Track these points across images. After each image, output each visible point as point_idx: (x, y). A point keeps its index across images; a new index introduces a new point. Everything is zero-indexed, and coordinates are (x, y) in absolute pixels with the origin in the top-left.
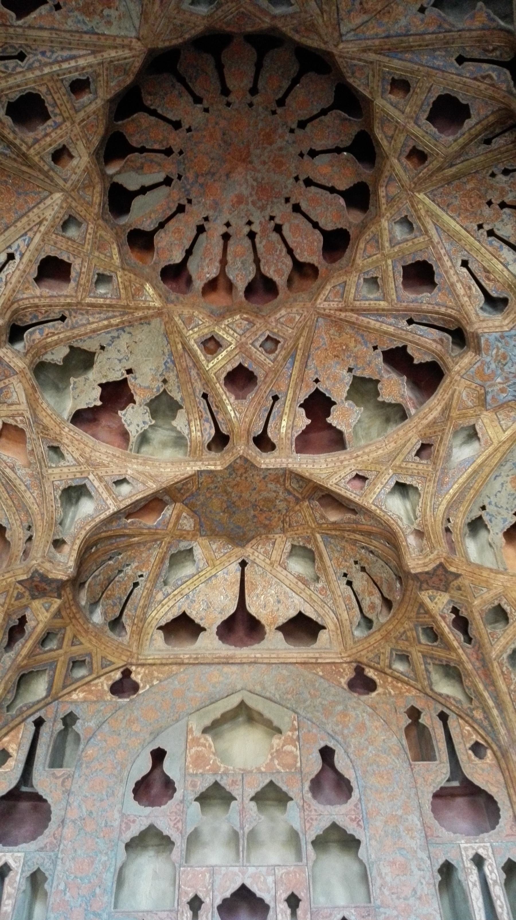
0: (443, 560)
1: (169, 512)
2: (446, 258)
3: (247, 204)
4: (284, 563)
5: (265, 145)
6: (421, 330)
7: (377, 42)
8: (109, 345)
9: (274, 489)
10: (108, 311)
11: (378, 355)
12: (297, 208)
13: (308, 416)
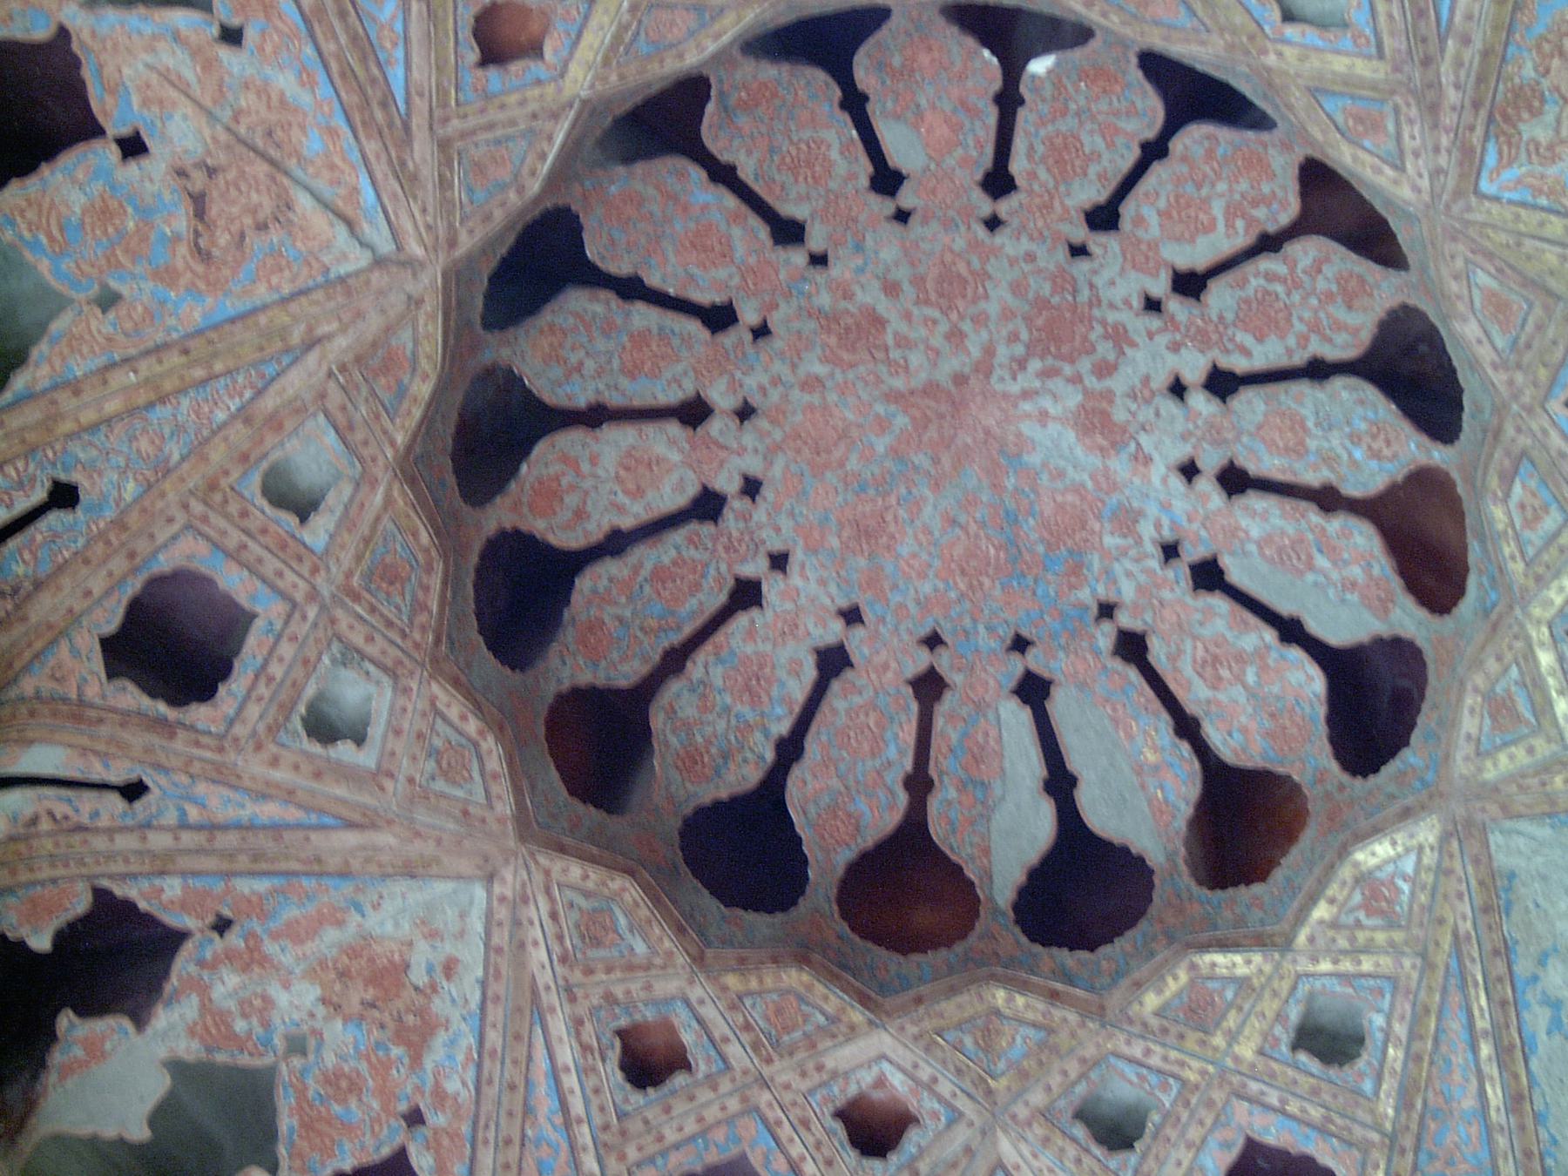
5: (890, 339)
7: (372, 147)
12: (1104, 218)
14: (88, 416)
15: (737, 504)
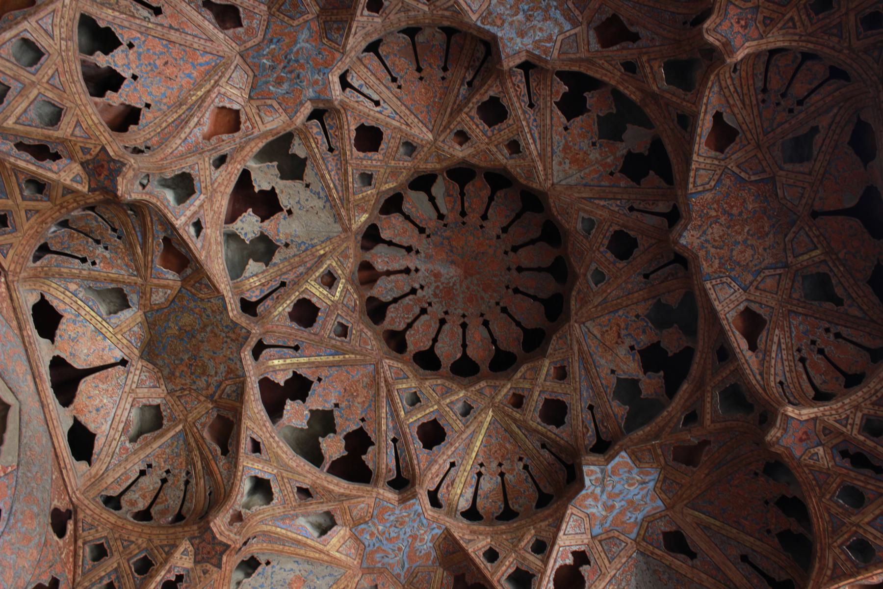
0: (233, 546)
1: (171, 277)
2: (453, 449)
3: (435, 282)
4: (138, 402)
6: (391, 452)
7: (586, 348)
8: (311, 191)
9: (219, 372)
10: (342, 186)
12: (443, 322)
13: (286, 382)
14: (641, 293)
15: (509, 249)
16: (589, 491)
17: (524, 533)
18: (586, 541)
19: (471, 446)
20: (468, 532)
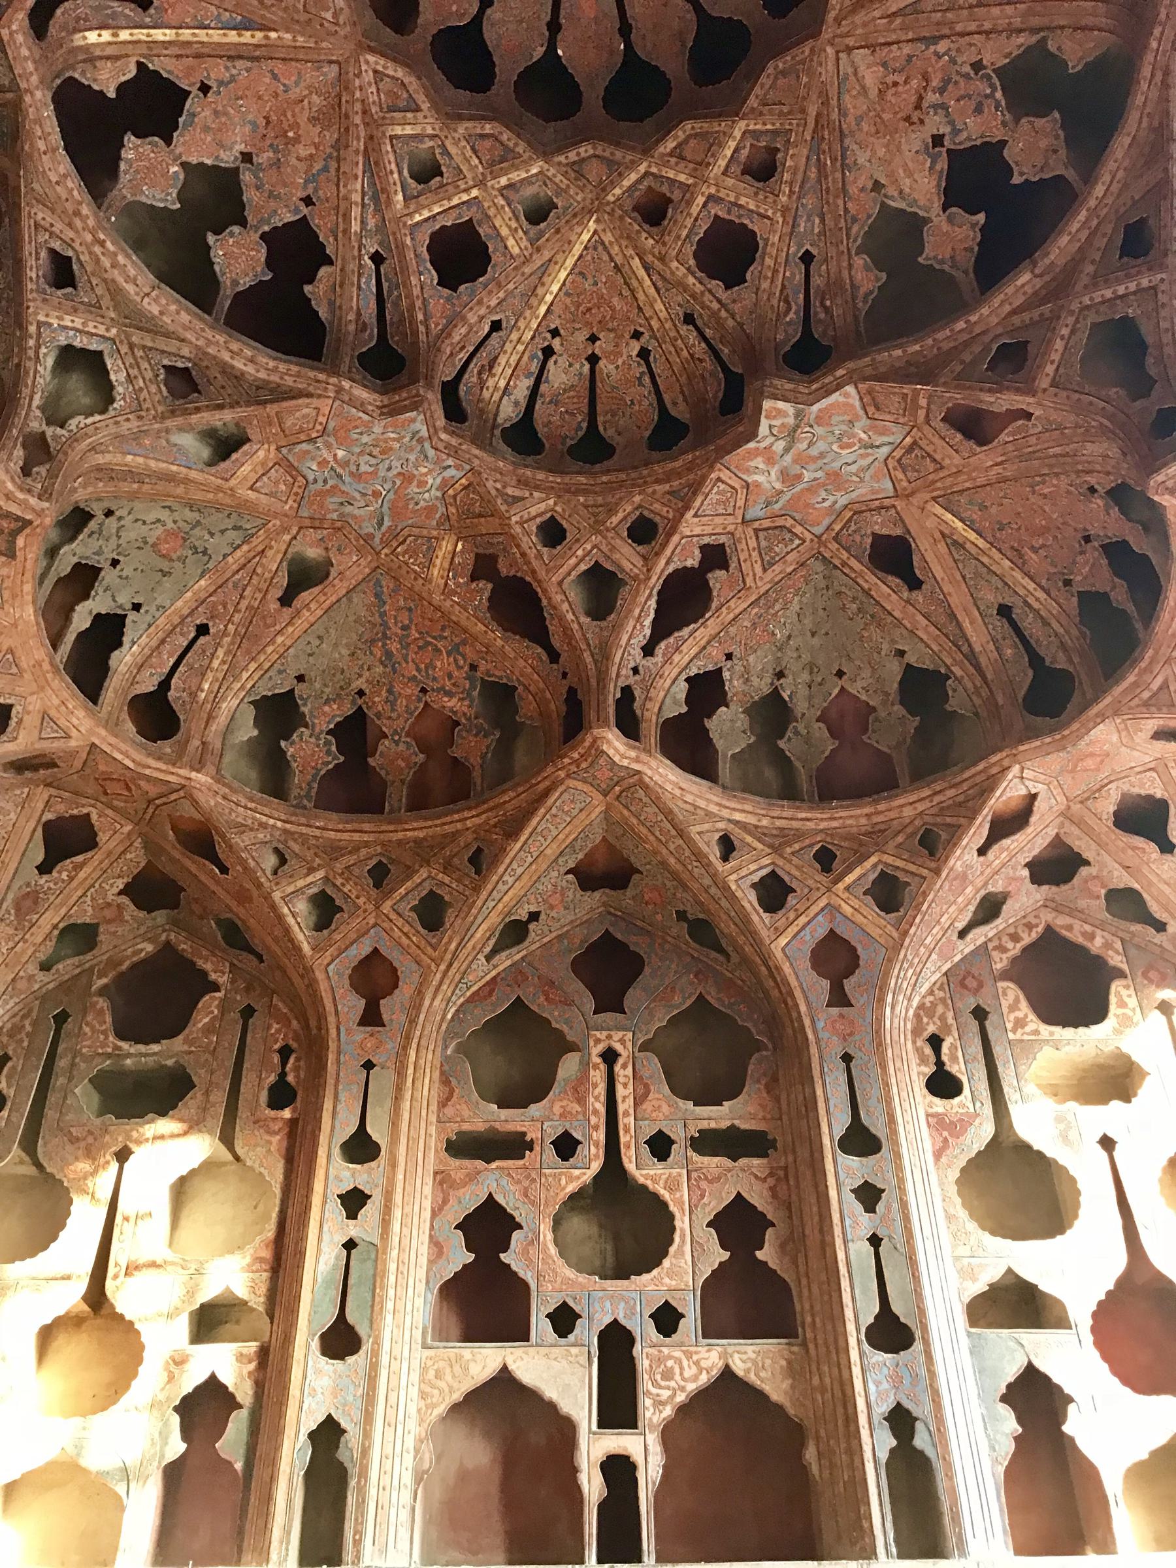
2: (501, 295)
6: (368, 283)
7: (835, 116)
11: (297, 210)
13: (121, 88)
16: (763, 445)
17: (621, 499)
18: (731, 528)
19: (540, 291)
20: (514, 483)
